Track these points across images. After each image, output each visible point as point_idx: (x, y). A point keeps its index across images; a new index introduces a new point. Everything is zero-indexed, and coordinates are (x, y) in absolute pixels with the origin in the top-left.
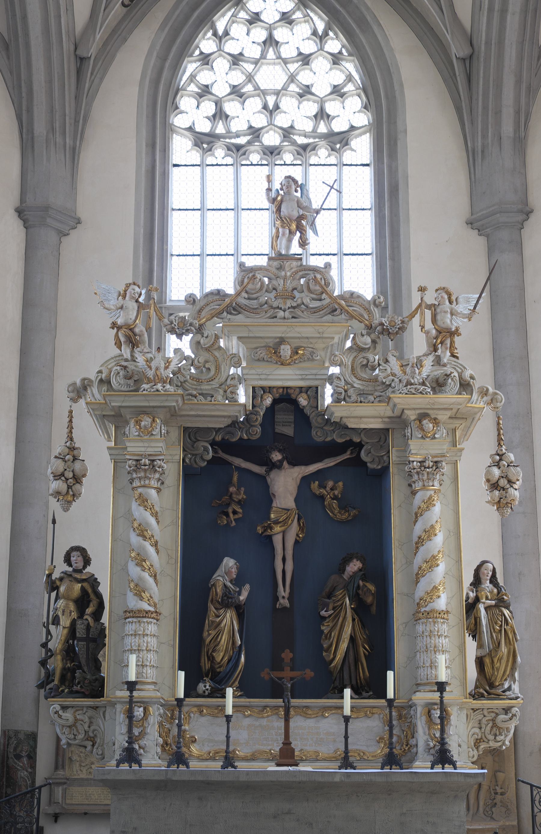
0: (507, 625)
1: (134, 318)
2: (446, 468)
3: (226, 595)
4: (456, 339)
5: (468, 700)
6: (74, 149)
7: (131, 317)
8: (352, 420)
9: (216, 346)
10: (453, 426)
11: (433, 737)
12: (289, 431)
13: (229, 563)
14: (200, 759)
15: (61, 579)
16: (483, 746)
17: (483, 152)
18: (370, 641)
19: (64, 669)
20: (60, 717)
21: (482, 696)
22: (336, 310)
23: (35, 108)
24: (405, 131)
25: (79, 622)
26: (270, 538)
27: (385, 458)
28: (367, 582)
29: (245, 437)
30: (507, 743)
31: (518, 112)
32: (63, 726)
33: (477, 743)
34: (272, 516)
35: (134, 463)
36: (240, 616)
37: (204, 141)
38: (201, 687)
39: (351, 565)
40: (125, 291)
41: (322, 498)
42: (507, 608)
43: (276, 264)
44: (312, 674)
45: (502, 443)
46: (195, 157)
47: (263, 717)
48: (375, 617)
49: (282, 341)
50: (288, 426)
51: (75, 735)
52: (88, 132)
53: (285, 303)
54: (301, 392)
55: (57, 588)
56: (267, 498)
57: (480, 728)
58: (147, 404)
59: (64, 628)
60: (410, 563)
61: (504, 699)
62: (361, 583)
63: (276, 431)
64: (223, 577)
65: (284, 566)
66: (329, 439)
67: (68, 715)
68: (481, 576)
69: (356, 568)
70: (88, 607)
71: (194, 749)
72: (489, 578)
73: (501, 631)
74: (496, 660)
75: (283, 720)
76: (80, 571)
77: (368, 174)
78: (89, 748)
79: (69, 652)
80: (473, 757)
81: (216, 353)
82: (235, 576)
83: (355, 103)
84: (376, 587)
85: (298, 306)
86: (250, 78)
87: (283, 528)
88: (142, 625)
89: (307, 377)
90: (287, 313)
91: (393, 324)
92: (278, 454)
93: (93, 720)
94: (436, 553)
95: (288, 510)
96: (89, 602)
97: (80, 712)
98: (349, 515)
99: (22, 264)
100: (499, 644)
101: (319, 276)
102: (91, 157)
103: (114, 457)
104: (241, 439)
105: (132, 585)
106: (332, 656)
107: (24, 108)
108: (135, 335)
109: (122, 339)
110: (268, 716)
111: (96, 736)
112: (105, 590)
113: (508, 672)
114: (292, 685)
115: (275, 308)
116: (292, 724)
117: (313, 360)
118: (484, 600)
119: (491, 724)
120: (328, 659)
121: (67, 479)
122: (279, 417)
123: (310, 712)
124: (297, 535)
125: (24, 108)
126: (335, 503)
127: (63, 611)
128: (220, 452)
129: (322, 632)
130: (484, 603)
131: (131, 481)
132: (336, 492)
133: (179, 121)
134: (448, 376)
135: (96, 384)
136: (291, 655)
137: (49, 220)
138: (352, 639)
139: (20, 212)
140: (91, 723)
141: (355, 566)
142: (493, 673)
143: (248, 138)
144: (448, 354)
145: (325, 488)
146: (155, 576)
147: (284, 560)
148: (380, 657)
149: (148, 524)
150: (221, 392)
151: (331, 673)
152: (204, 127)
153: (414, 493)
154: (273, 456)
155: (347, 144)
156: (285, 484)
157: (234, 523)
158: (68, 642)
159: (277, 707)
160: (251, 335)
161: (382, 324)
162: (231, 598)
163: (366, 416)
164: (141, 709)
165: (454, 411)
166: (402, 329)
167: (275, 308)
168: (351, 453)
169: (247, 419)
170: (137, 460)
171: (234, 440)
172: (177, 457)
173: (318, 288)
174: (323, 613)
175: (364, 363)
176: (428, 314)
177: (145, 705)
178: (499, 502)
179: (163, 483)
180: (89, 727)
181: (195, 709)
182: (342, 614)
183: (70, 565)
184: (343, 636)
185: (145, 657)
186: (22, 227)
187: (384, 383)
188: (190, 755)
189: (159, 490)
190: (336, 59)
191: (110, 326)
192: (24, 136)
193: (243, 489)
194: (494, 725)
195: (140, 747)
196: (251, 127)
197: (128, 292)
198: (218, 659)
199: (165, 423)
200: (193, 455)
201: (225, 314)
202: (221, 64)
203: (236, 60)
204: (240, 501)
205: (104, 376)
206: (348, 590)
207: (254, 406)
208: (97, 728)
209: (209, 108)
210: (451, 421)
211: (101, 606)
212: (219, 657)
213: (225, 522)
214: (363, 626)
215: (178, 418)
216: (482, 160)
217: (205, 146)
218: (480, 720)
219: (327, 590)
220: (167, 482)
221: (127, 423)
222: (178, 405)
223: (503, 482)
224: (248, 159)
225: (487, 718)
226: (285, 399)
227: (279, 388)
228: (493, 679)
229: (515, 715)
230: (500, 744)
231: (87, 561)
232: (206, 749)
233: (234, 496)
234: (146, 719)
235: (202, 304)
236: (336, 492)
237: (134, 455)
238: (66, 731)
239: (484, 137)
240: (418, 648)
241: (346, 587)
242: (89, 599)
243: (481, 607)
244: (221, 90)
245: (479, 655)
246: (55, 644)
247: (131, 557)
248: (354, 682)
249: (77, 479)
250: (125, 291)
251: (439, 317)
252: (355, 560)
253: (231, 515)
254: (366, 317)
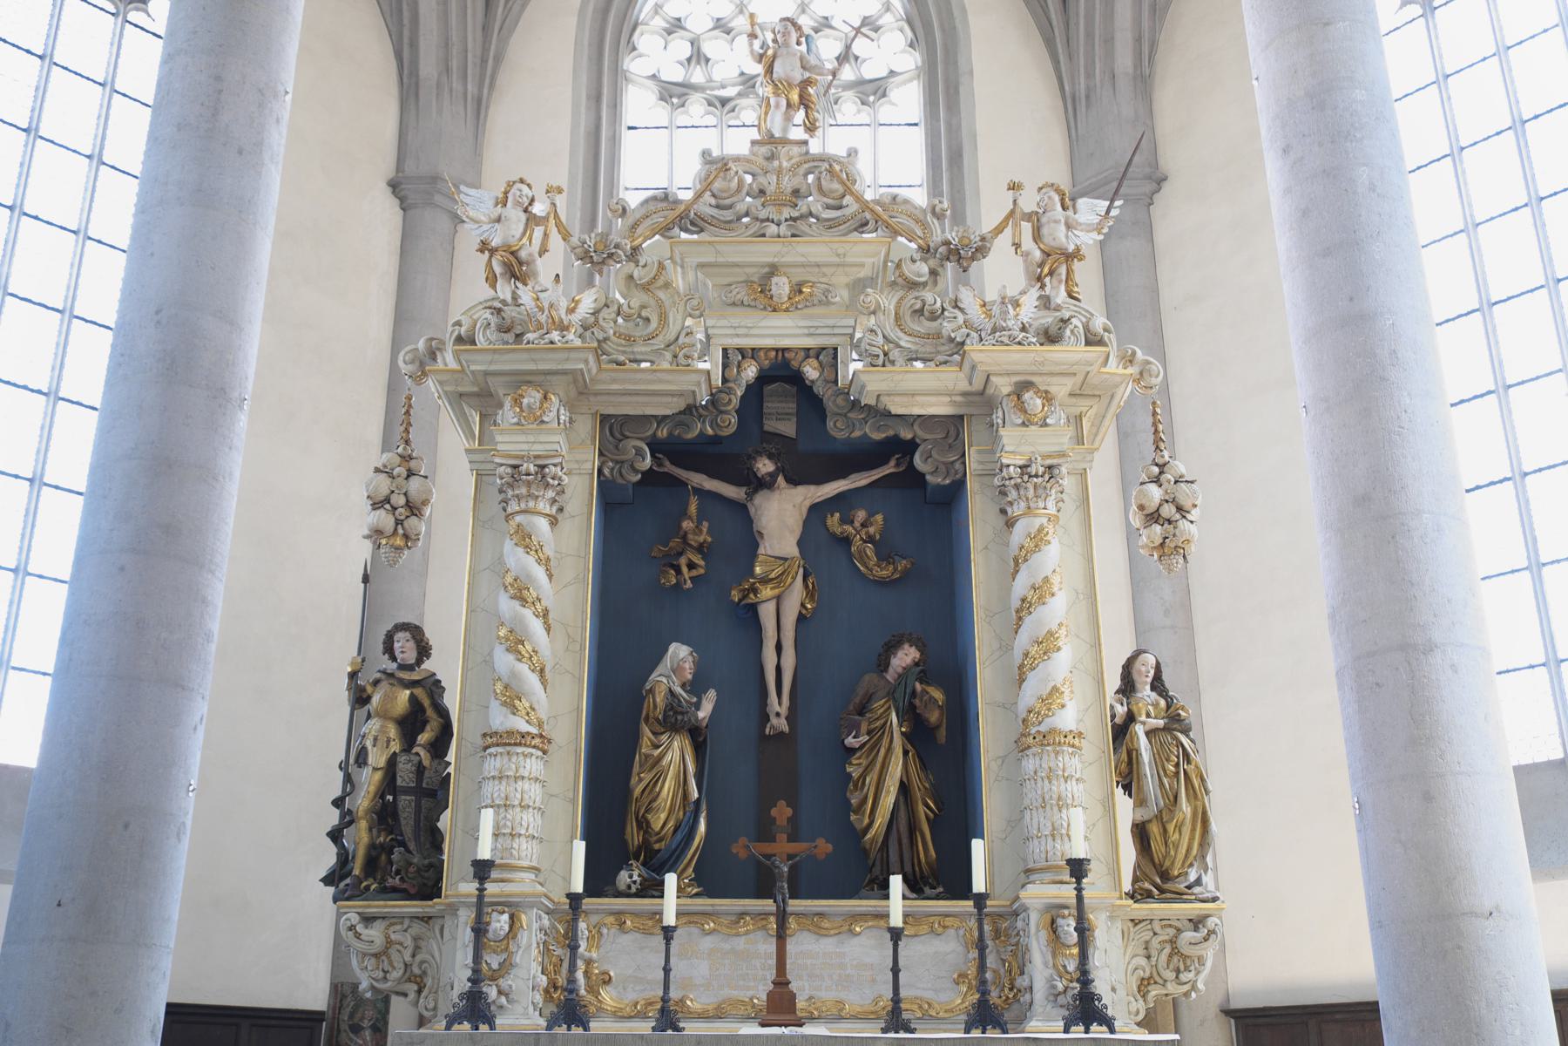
0: (1189, 762)
1: (518, 236)
2: (1068, 482)
3: (672, 708)
4: (1076, 265)
5: (1124, 902)
6: (479, 101)
7: (513, 232)
8: (897, 399)
9: (660, 282)
10: (1077, 411)
11: (1062, 972)
12: (788, 428)
13: (679, 652)
14: (618, 1016)
15: (376, 683)
16: (1154, 992)
17: (1087, 97)
18: (936, 793)
19: (372, 846)
20: (358, 936)
21: (1149, 895)
22: (866, 224)
23: (421, 39)
24: (971, 73)
25: (402, 759)
26: (753, 609)
27: (958, 466)
28: (928, 684)
29: (710, 431)
30: (1200, 985)
31: (1138, 40)
32: (365, 955)
33: (1144, 985)
34: (758, 570)
35: (509, 470)
36: (699, 748)
37: (673, 93)
38: (623, 878)
39: (900, 654)
40: (506, 193)
41: (846, 541)
42: (1186, 732)
43: (764, 150)
44: (830, 847)
45: (1162, 446)
46: (661, 114)
47: (738, 935)
48: (945, 749)
49: (774, 270)
50: (786, 415)
51: (385, 972)
52: (501, 79)
53: (781, 213)
54: (808, 357)
55: (368, 700)
56: (750, 540)
57: (1149, 957)
58: (532, 367)
59: (375, 769)
60: (1006, 648)
61: (1190, 901)
62: (918, 686)
63: (766, 428)
64: (668, 677)
65: (780, 658)
66: (857, 434)
67: (375, 933)
68: (1135, 676)
69: (908, 660)
70: (422, 730)
71: (607, 996)
72: (1149, 680)
73: (1177, 773)
74: (1171, 827)
75: (774, 940)
76: (410, 668)
78: (412, 996)
79: (384, 815)
80: (1138, 1013)
81: (661, 294)
82: (690, 677)
84: (947, 693)
85: (802, 217)
87: (777, 591)
88: (514, 759)
89: (820, 331)
90: (783, 228)
91: (966, 241)
92: (767, 461)
93: (422, 944)
94: (1054, 627)
95: (786, 559)
96: (425, 722)
97: (398, 927)
98: (895, 569)
99: (396, 259)
100: (1176, 797)
101: (837, 168)
102: (504, 115)
103: (476, 466)
104: (702, 434)
105: (499, 687)
106: (866, 821)
107: (406, 40)
108: (521, 263)
109: (498, 269)
110: (747, 933)
111: (425, 973)
112: (452, 701)
113: (1195, 851)
114: (791, 868)
115: (763, 221)
116: (791, 947)
117: (828, 303)
118: (1143, 718)
119: (1168, 950)
120: (858, 827)
121: (394, 509)
122: (770, 406)
123: (826, 924)
124: (803, 605)
125: (406, 40)
126: (869, 549)
127: (375, 739)
128: (667, 463)
129: (849, 775)
130: (1144, 723)
131: (505, 501)
132: (872, 530)
133: (635, 66)
134: (1065, 321)
135: (450, 347)
136: (789, 812)
137: (438, 198)
138: (904, 788)
139: (394, 186)
140: (417, 949)
141: (906, 656)
142: (1167, 853)
143: (738, 89)
144: (1063, 293)
145: (852, 522)
146: (542, 671)
147: (779, 648)
148: (956, 816)
149: (529, 576)
150: (668, 356)
151: (865, 852)
152: (675, 74)
153: (1010, 524)
154: (760, 465)
155: (884, 95)
157: (689, 585)
158: (382, 797)
159: (764, 915)
160: (721, 260)
161: (947, 243)
162: (682, 713)
164: (506, 917)
165: (1079, 378)
166: (981, 251)
167: (763, 221)
168: (897, 465)
169: (714, 401)
170: (515, 467)
171: (690, 436)
172: (588, 466)
173: (836, 186)
174: (850, 741)
175: (918, 306)
176: (1026, 227)
177: (513, 908)
178: (1162, 545)
179: (561, 510)
180: (413, 956)
181: (611, 919)
182: (885, 742)
183: (394, 659)
184: (887, 780)
186: (398, 209)
187: (952, 340)
188: (600, 1009)
189: (554, 522)
191: (477, 247)
192: (405, 80)
193: (706, 524)
194: (1175, 952)
195: (500, 992)
196: (742, 74)
197: (510, 196)
198: (657, 826)
199: (570, 405)
200: (617, 462)
201: (677, 230)
204: (701, 545)
205: (463, 330)
206: (895, 700)
207: (725, 380)
208: (427, 957)
210: (1073, 400)
211: (446, 731)
212: (658, 820)
213: (674, 581)
214: (924, 766)
215: (592, 399)
216: (1088, 107)
217: (675, 100)
218: (1147, 942)
219: (857, 700)
220: (568, 509)
221: (500, 406)
222: (589, 371)
223: (1168, 511)
224: (737, 117)
225: (1161, 938)
227: (768, 350)
228: (1167, 863)
229: (1214, 932)
230: (1186, 988)
231: (424, 651)
232: (631, 996)
233: (690, 536)
234: (514, 937)
235: (638, 216)
236: (872, 530)
237: (510, 457)
238: (370, 963)
239: (1090, 75)
240: (1027, 802)
241: (891, 694)
242: (425, 720)
243: (1139, 730)
245: (1139, 819)
246: (362, 801)
247: (499, 637)
248: (908, 868)
249: (413, 509)
250: (506, 193)
251: (1045, 231)
252: (906, 646)
253: (685, 569)
254: (919, 233)
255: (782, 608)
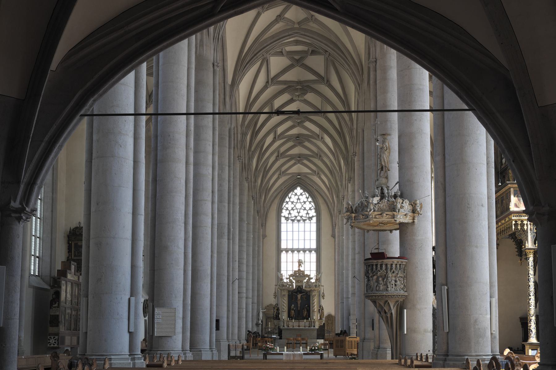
37: (287, 219)
46: (286, 221)
48: (309, 311)
65: (299, 305)
77: (315, 224)
83: (313, 211)
86: (295, 206)
133: (283, 215)
148: (309, 316)
152: (287, 216)
156: (299, 296)
163: (308, 289)
184: (305, 313)
185: (284, 316)
190: (310, 202)
202: (290, 203)
203: (292, 202)
209: (288, 212)
226: (299, 286)
244: (290, 209)
255: (299, 302)
